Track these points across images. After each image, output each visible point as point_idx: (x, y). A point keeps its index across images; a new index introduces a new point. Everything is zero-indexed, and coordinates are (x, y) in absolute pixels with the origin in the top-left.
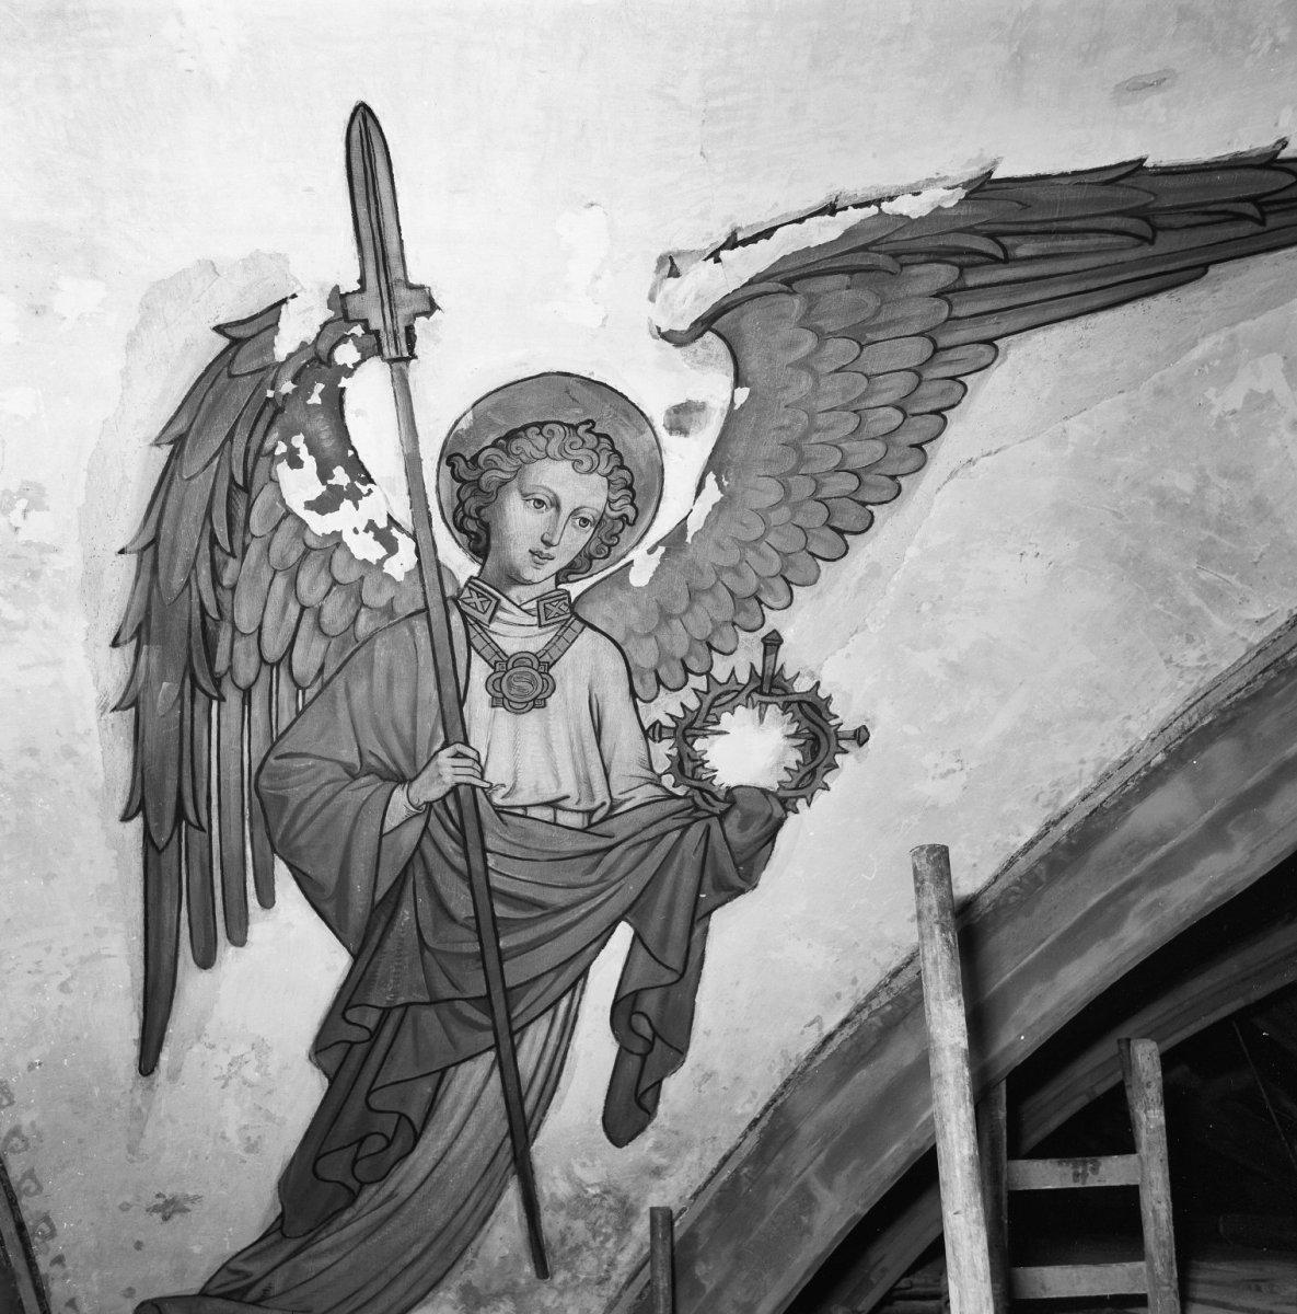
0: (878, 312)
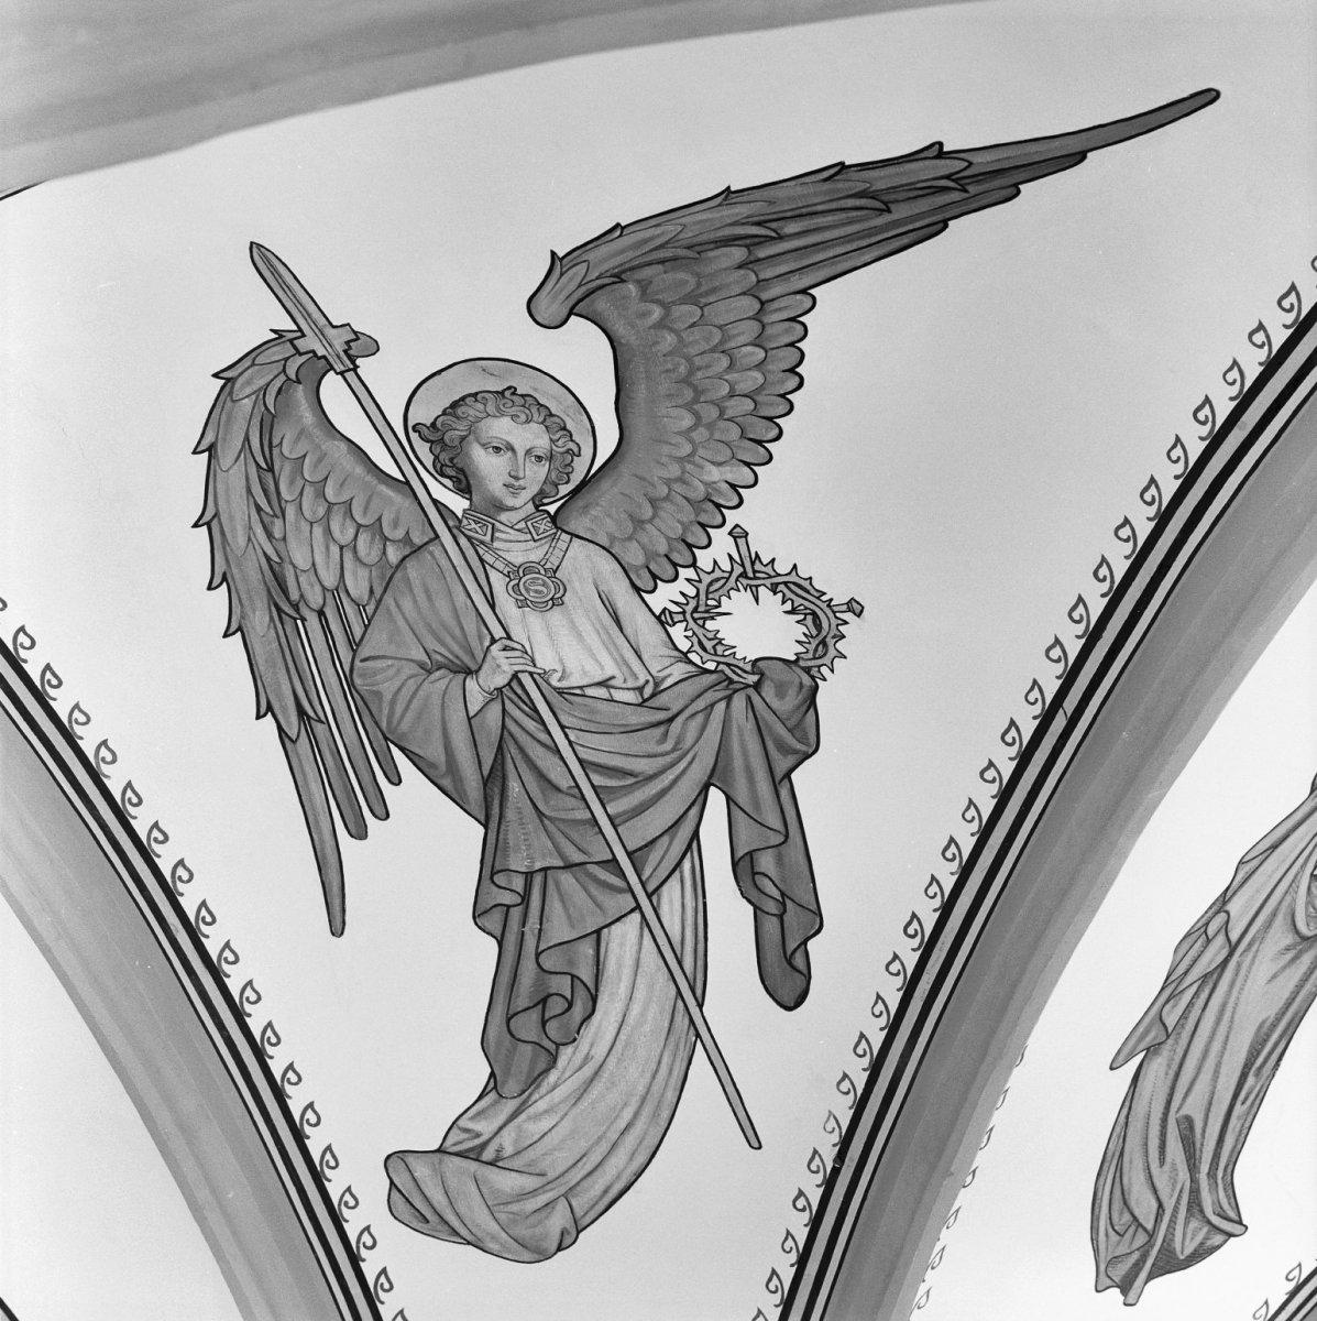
0: (699, 285)
